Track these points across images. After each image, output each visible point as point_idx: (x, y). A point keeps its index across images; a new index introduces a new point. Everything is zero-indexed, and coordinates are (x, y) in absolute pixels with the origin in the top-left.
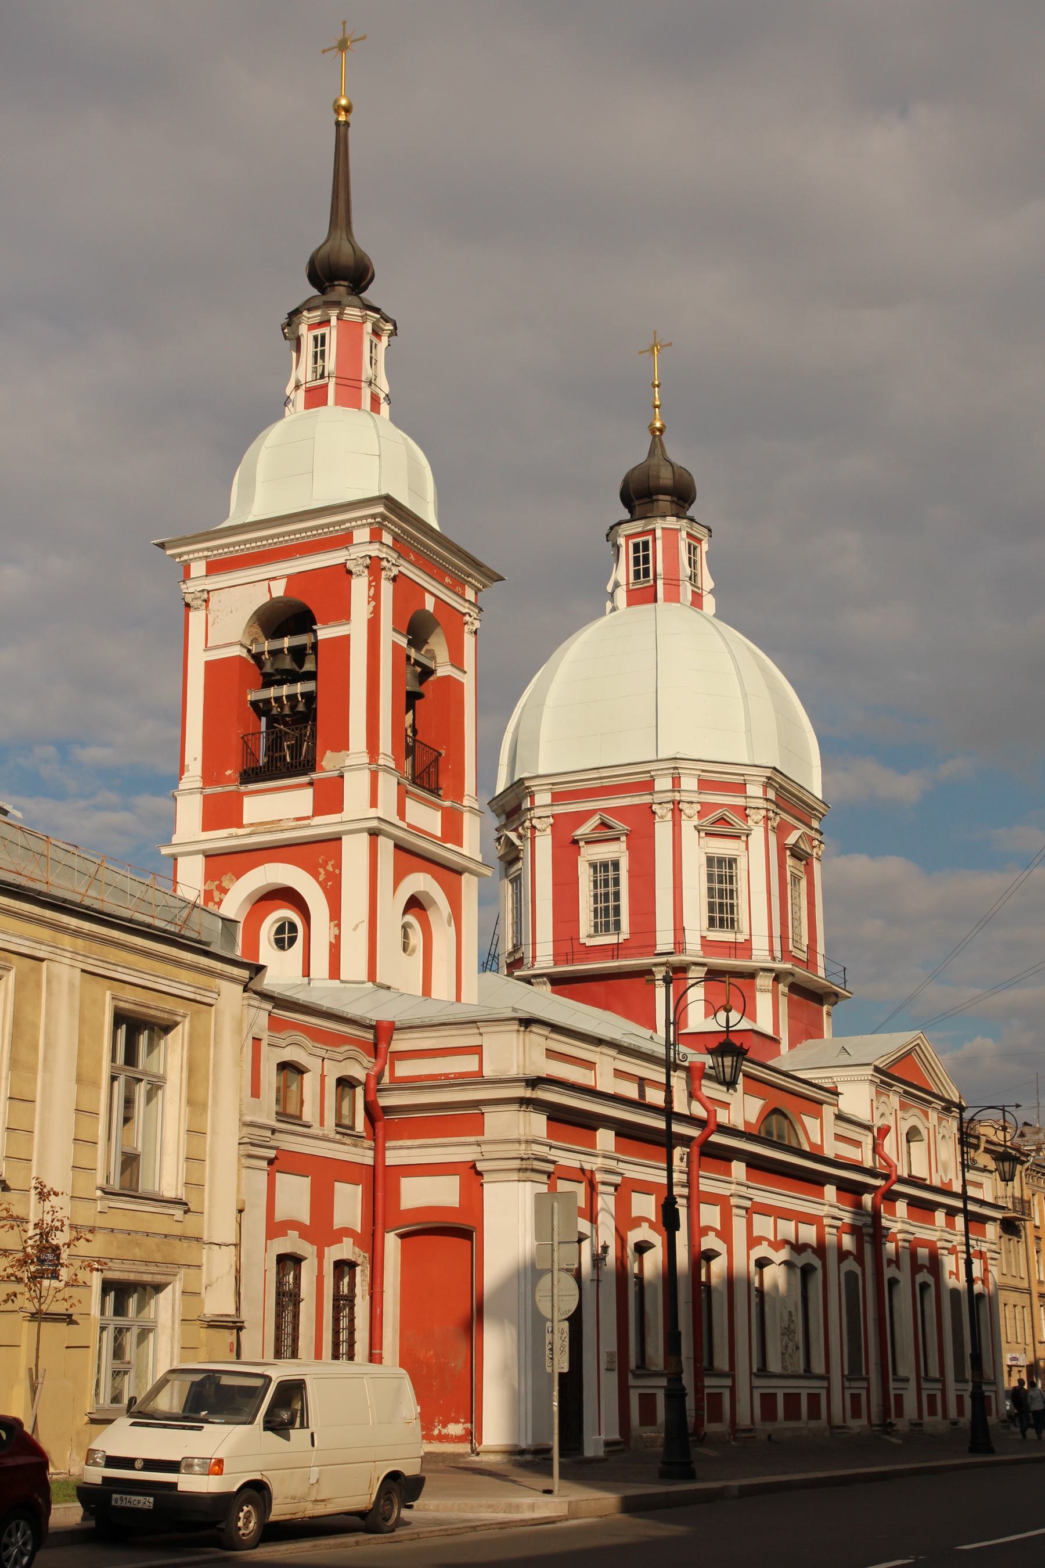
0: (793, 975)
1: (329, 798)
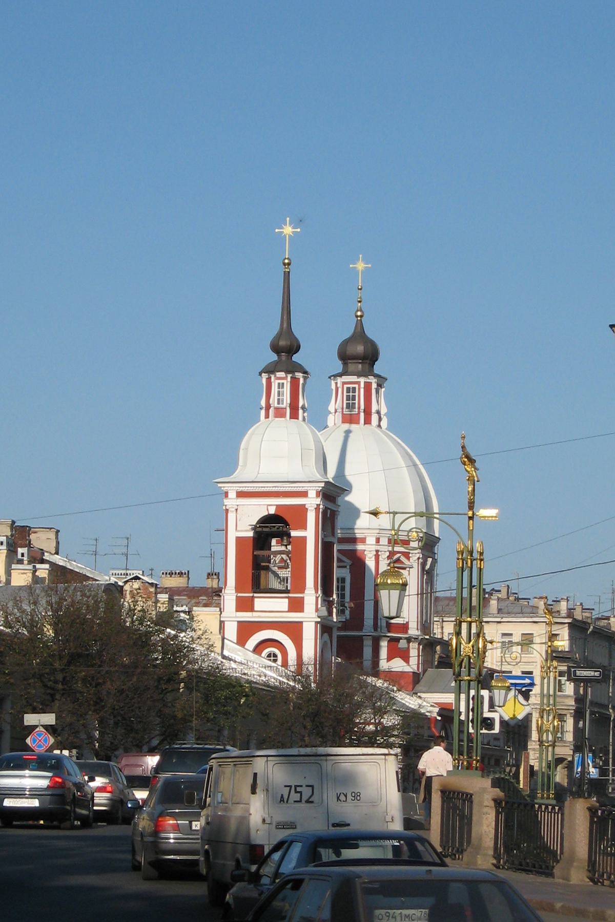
1: (297, 605)
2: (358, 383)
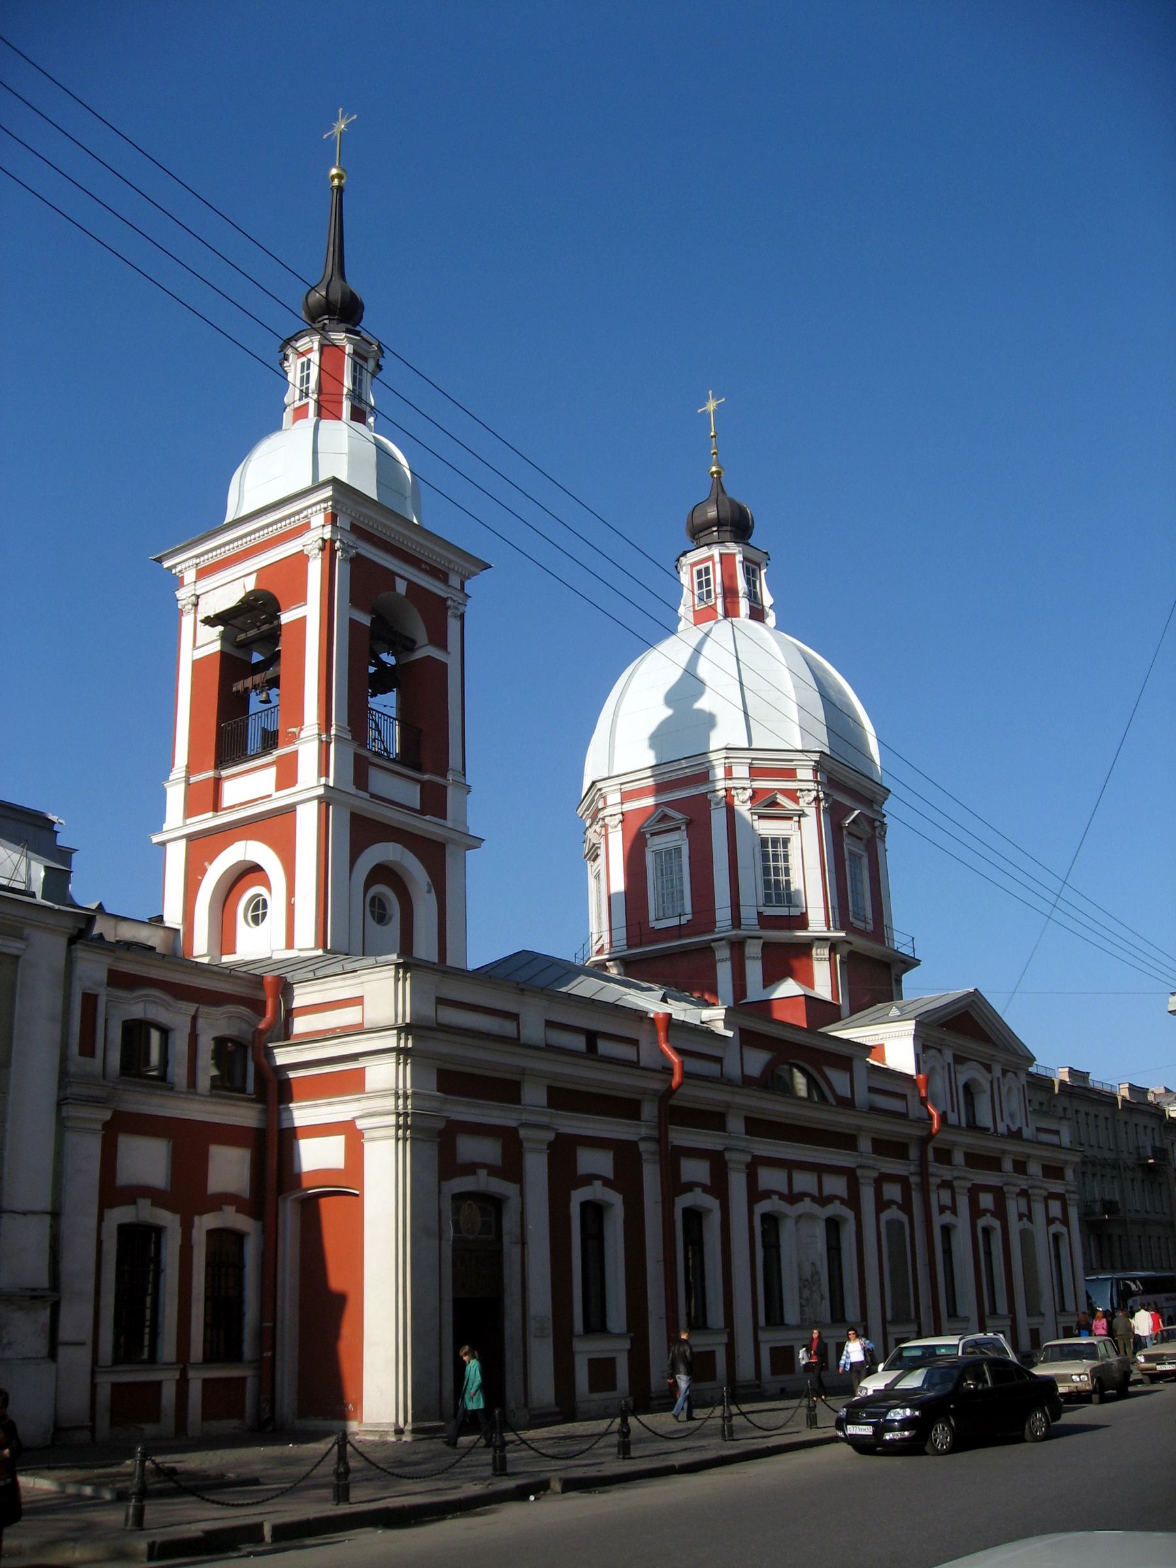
0: (850, 943)
2: (711, 558)
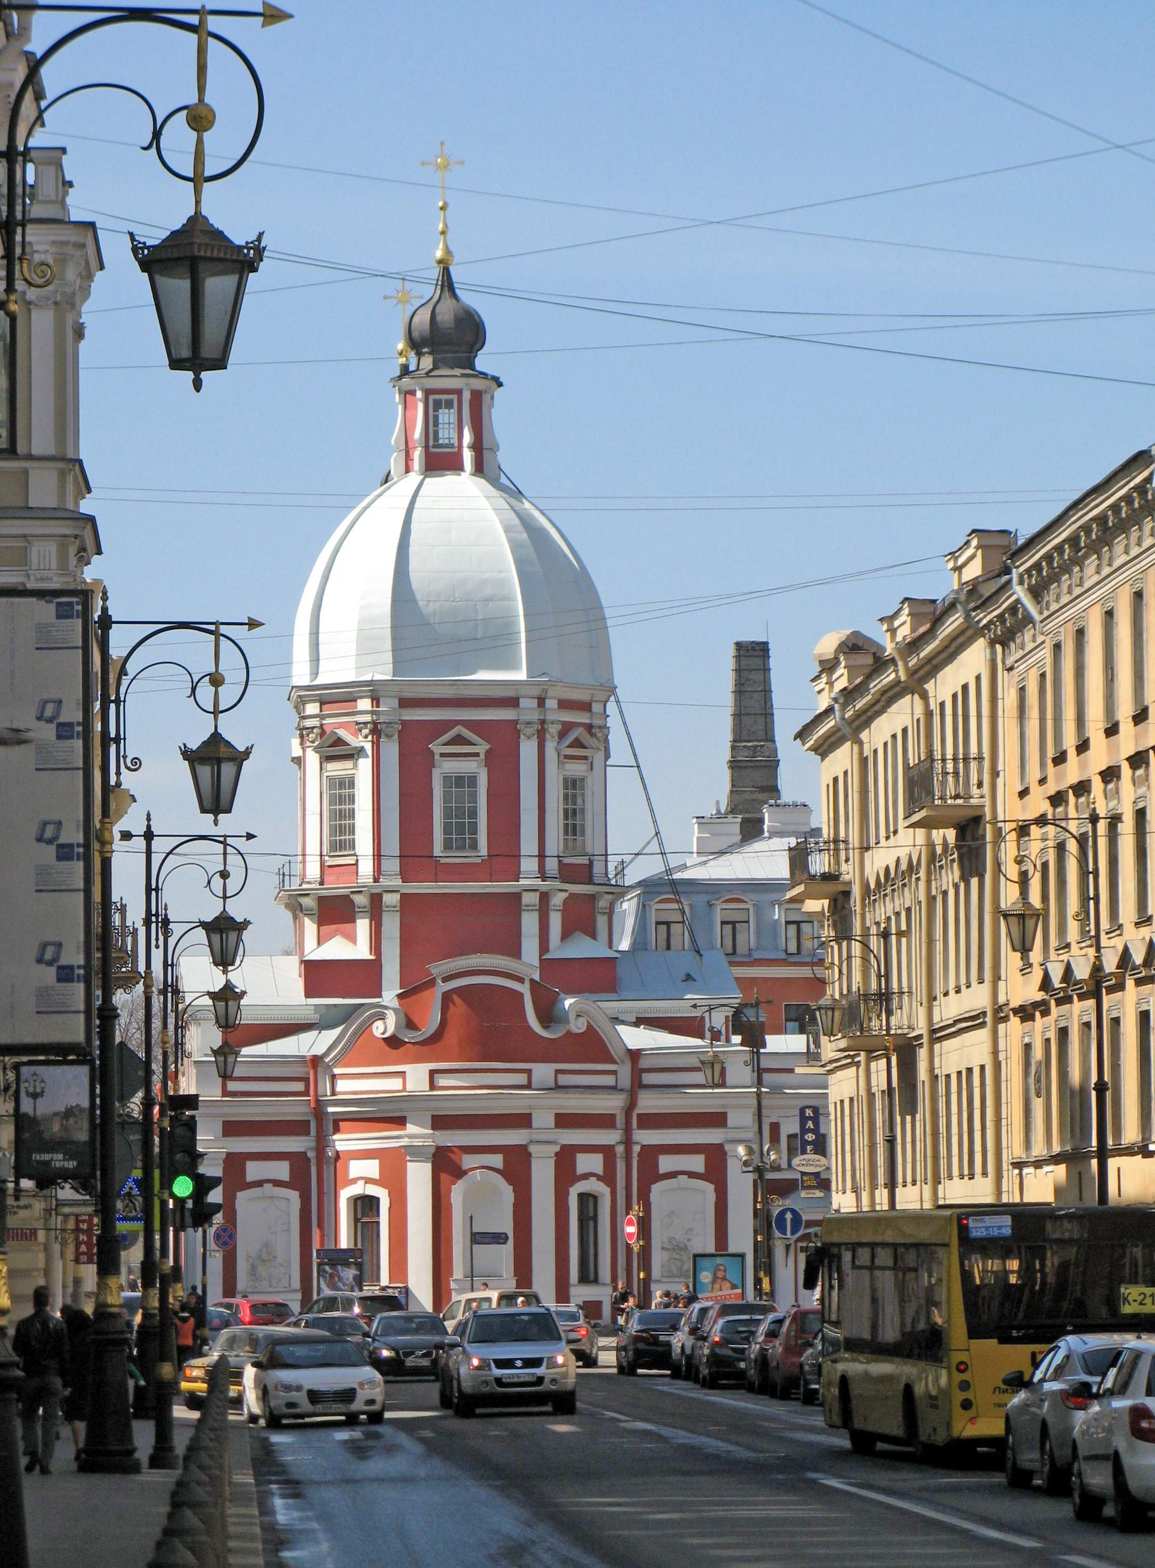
2: (459, 392)
